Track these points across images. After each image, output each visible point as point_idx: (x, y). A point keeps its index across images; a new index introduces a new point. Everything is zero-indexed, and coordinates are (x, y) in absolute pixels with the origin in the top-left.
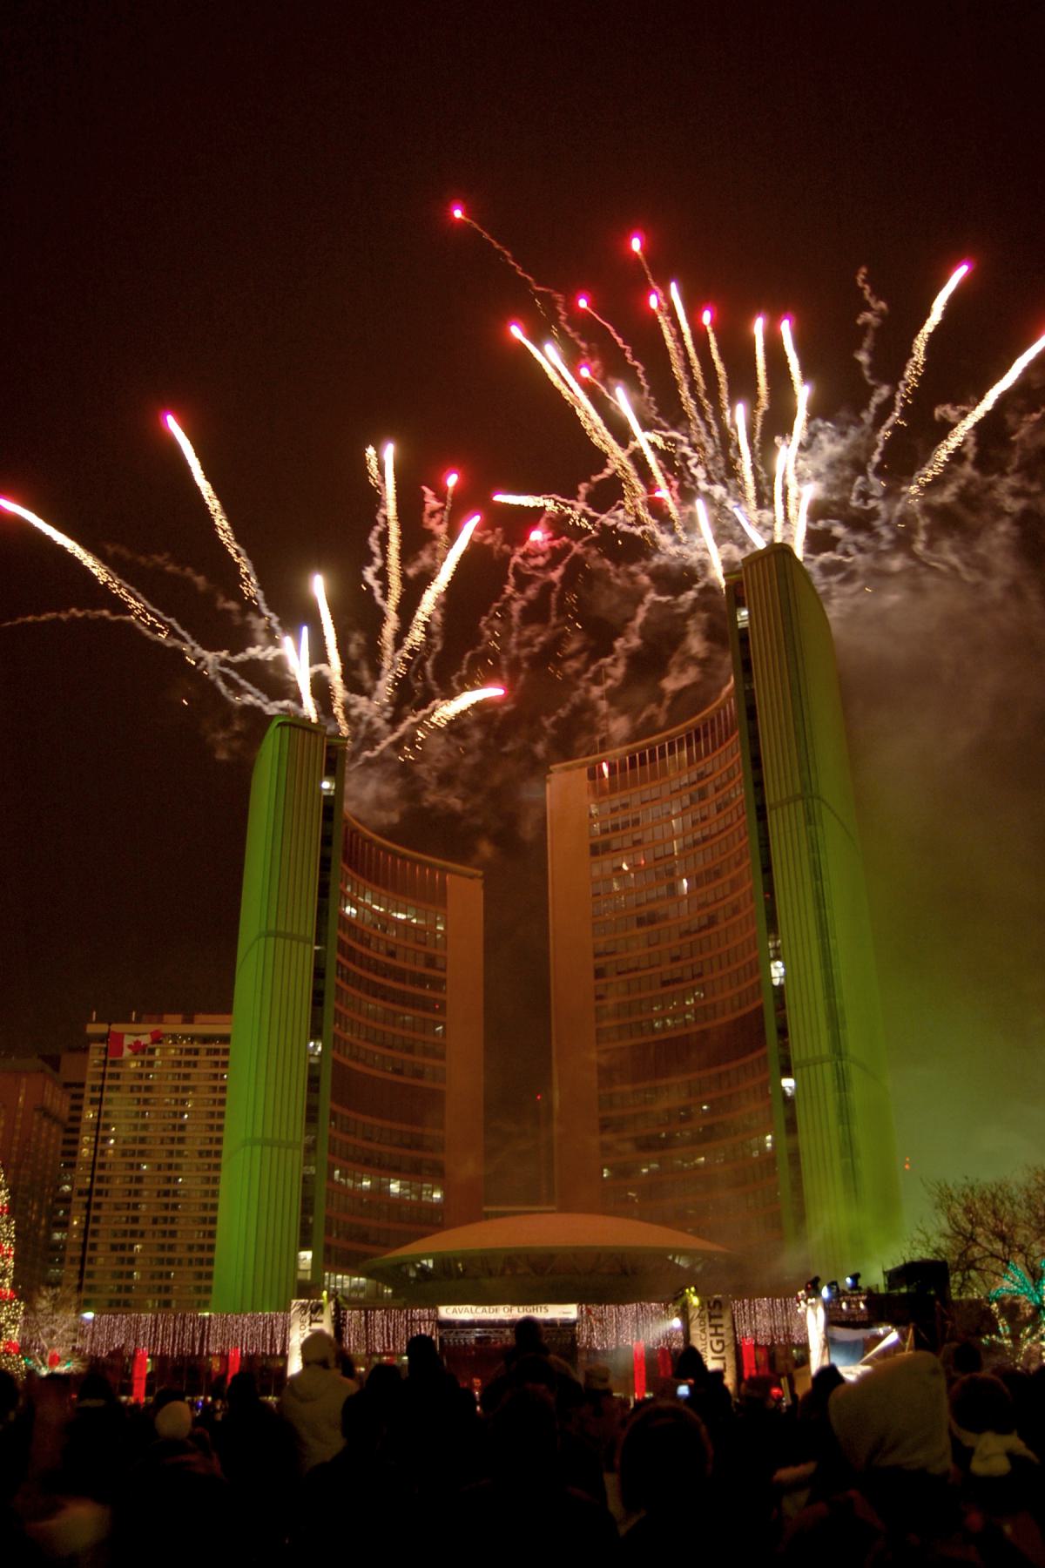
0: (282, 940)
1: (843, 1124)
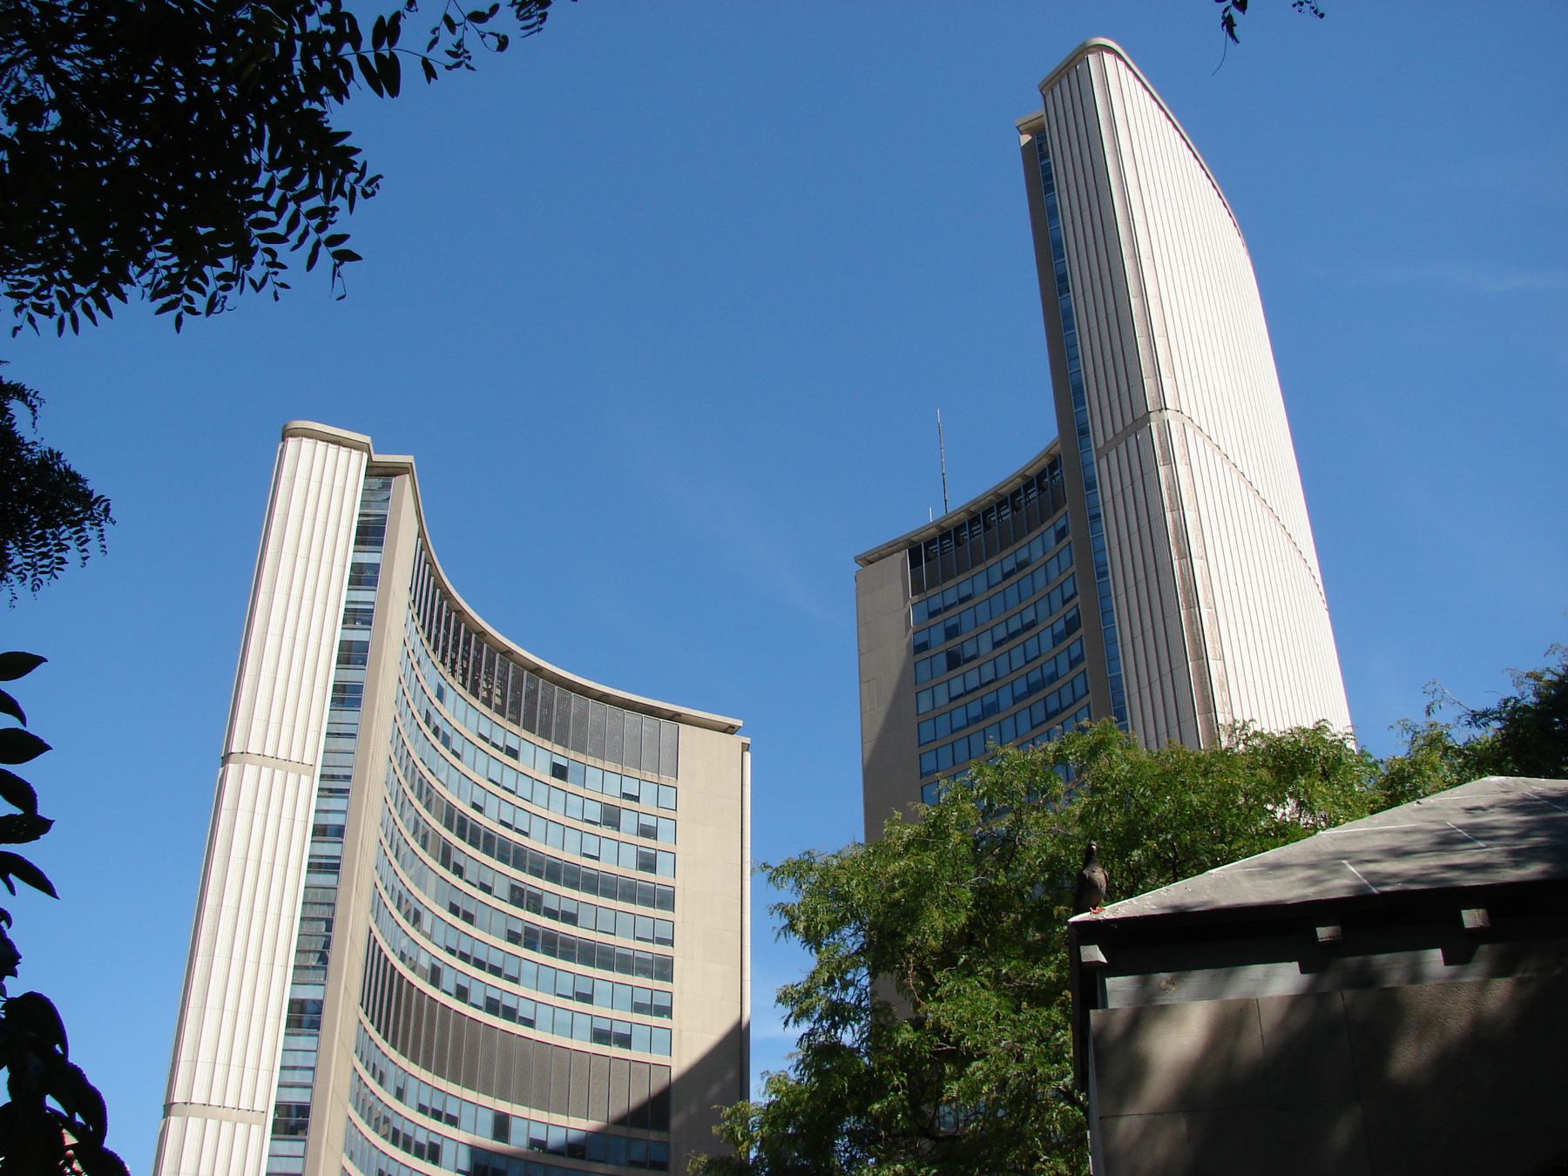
0: (255, 769)
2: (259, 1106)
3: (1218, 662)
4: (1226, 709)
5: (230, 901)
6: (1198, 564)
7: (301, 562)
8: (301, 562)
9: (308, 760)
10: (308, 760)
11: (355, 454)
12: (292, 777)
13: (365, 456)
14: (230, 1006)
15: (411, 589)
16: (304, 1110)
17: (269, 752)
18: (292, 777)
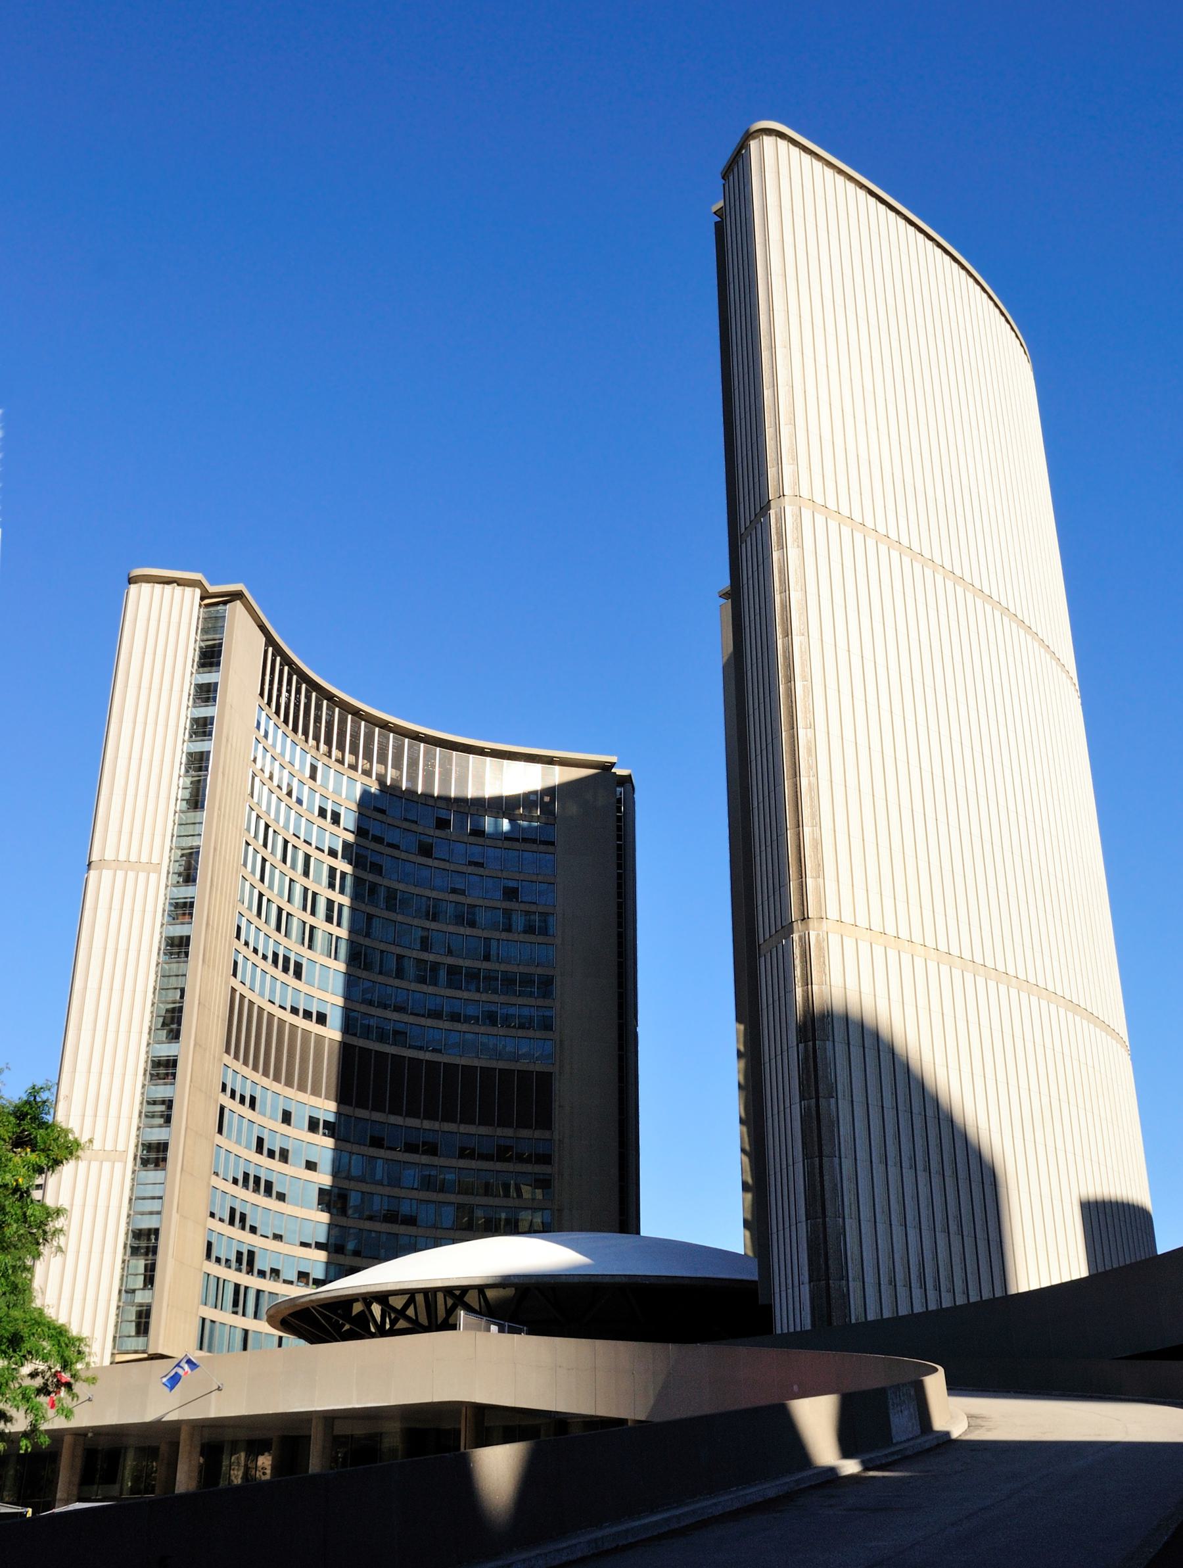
1: (806, 1042)
2: (120, 1147)
3: (809, 730)
4: (811, 773)
5: (93, 983)
6: (797, 640)
7: (144, 692)
8: (144, 692)
9: (155, 860)
10: (155, 860)
11: (188, 590)
12: (142, 876)
13: (198, 592)
14: (95, 1069)
15: (262, 694)
16: (163, 1147)
17: (122, 857)
18: (142, 876)
